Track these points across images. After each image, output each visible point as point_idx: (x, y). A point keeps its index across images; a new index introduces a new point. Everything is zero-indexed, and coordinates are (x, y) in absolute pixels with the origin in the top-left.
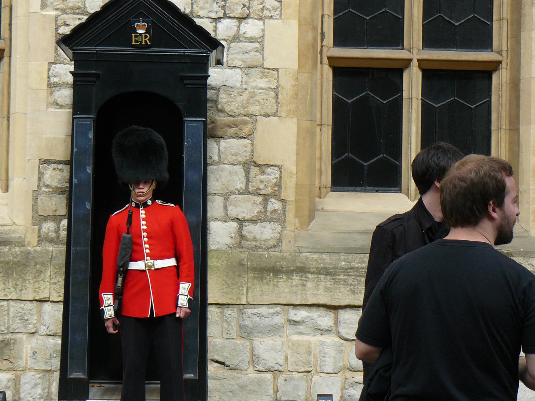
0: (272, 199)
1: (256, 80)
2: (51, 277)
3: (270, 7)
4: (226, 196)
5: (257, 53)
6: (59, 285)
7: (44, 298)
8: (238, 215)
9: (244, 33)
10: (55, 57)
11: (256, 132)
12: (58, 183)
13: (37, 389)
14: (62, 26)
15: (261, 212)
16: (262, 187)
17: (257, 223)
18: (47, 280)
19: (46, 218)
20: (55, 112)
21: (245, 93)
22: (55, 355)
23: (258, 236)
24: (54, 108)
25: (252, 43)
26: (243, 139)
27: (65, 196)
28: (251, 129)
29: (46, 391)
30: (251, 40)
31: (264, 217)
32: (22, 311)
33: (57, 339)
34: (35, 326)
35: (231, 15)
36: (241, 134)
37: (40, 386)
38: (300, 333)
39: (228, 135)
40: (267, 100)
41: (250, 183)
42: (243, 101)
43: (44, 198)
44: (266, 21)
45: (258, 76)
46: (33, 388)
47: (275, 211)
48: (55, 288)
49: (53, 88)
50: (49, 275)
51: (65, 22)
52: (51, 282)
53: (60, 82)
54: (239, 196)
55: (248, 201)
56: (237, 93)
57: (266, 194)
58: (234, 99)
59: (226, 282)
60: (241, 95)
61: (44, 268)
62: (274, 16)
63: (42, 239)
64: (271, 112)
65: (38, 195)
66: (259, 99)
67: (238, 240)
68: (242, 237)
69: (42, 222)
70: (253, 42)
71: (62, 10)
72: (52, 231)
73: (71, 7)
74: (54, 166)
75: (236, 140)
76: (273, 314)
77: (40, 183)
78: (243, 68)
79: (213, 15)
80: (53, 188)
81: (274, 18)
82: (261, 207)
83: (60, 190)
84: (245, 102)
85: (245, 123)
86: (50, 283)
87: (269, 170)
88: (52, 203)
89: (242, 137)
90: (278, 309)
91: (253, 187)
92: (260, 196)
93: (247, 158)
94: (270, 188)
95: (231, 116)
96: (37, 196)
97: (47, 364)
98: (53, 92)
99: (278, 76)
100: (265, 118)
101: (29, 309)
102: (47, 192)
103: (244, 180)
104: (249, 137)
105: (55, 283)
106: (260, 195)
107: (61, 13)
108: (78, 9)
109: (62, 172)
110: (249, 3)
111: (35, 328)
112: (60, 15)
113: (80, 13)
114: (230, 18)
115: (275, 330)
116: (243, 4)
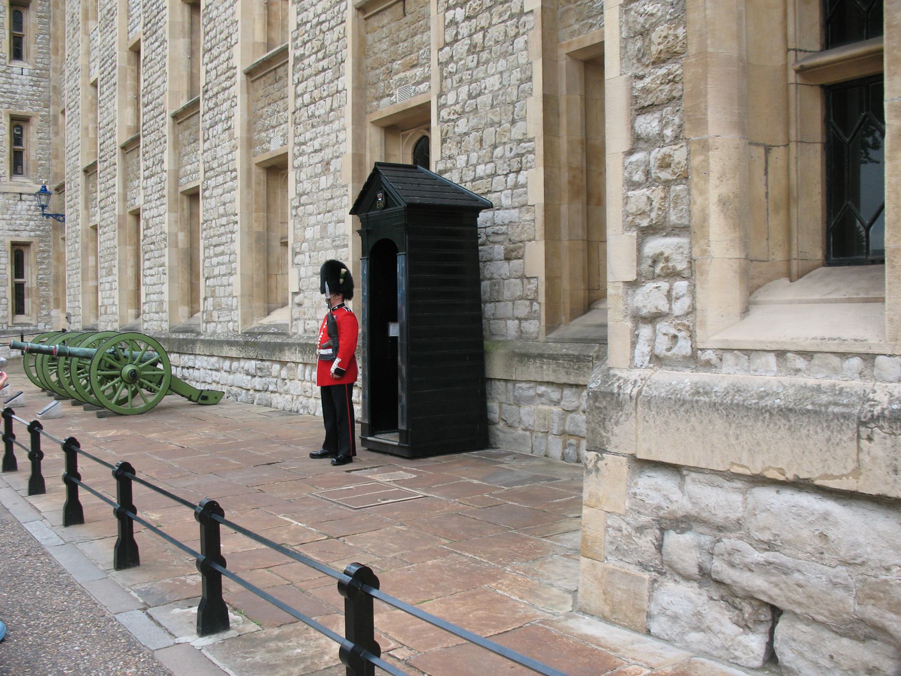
4: (513, 301)
38: (543, 404)
47: (535, 311)
68: (521, 331)
79: (505, 172)
85: (520, 248)
87: (532, 281)
90: (532, 385)
95: (514, 243)
114: (513, 172)
115: (530, 400)
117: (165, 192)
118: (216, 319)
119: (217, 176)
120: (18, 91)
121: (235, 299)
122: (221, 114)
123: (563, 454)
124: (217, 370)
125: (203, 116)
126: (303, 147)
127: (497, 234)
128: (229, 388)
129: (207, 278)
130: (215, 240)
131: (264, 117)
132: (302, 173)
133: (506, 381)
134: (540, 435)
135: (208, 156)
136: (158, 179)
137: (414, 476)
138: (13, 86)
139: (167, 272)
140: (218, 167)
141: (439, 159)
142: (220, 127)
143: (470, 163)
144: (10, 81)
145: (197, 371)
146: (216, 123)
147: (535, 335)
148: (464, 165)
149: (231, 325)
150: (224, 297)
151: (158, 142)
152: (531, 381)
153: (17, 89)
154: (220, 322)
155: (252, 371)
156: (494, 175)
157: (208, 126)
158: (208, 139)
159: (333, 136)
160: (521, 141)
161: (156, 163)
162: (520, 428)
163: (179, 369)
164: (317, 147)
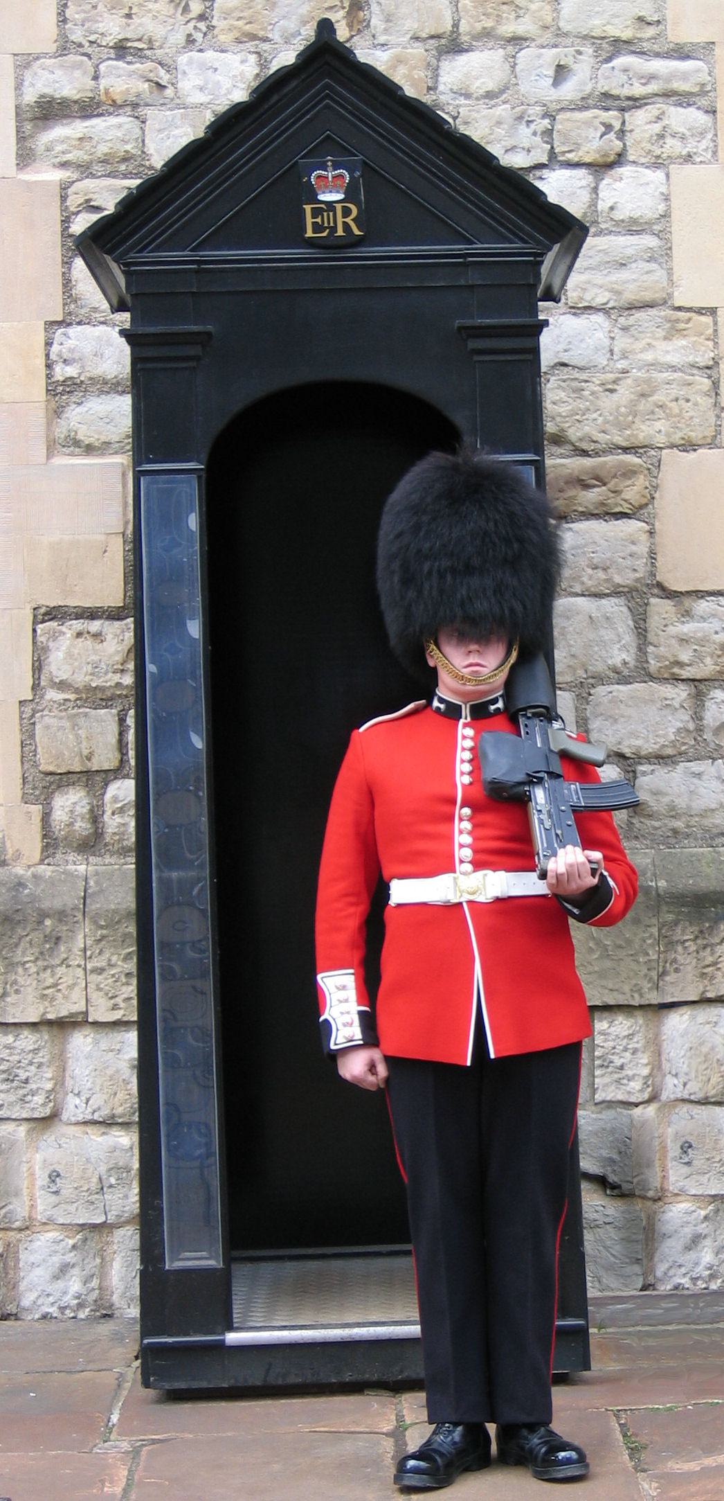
0: (716, 691)
1: (654, 343)
2: (89, 953)
3: (682, 130)
5: (654, 266)
6: (113, 976)
7: (72, 1015)
8: (620, 743)
9: (612, 208)
10: (64, 305)
11: (661, 497)
12: (91, 674)
13: (69, 1280)
14: (79, 212)
15: (688, 731)
16: (685, 657)
17: (675, 763)
18: (76, 963)
19: (62, 780)
20: (73, 465)
21: (621, 382)
22: (113, 1181)
23: (682, 803)
24: (69, 455)
25: (637, 237)
26: (624, 520)
27: (114, 711)
28: (647, 488)
29: (95, 1283)
30: (634, 227)
31: (697, 747)
32: (11, 1055)
33: (117, 1133)
34: (52, 1097)
35: (570, 156)
36: (617, 505)
37: (76, 1271)
39: (581, 509)
40: (688, 401)
41: (650, 649)
42: (618, 407)
43: (53, 722)
44: (673, 168)
45: (661, 333)
46: (56, 1277)
48: (102, 986)
49: (64, 397)
50: (83, 946)
51: (88, 201)
52: (89, 967)
53: (82, 379)
54: (621, 687)
55: (646, 702)
56: (599, 385)
57: (698, 677)
58: (591, 401)
59: (598, 942)
60: (612, 391)
61: (65, 928)
62: (695, 153)
63: (51, 843)
64: (700, 436)
65: (34, 712)
66: (663, 398)
69: (52, 793)
70: (638, 232)
71: (80, 166)
72: (82, 818)
73: (106, 155)
74: (78, 625)
75: (604, 523)
77: (39, 678)
78: (612, 311)
80: (77, 691)
81: (698, 160)
82: (687, 718)
83: (99, 696)
84: (623, 410)
85: (629, 473)
86: (85, 969)
87: (703, 606)
88: (77, 736)
89: (621, 513)
91: (659, 658)
92: (682, 686)
93: (637, 575)
94: (708, 660)
95: (584, 453)
96: (33, 716)
97: (92, 1208)
98: (63, 407)
99: (716, 331)
100: (685, 454)
101: (31, 1048)
102: (60, 705)
103: (629, 638)
104: (642, 512)
105: (100, 971)
106: (683, 680)
107: (75, 176)
108: (125, 160)
109: (102, 641)
110: (621, 121)
111: (51, 1104)
112: (74, 182)
113: (131, 173)
116: (603, 124)
160: (619, 46)
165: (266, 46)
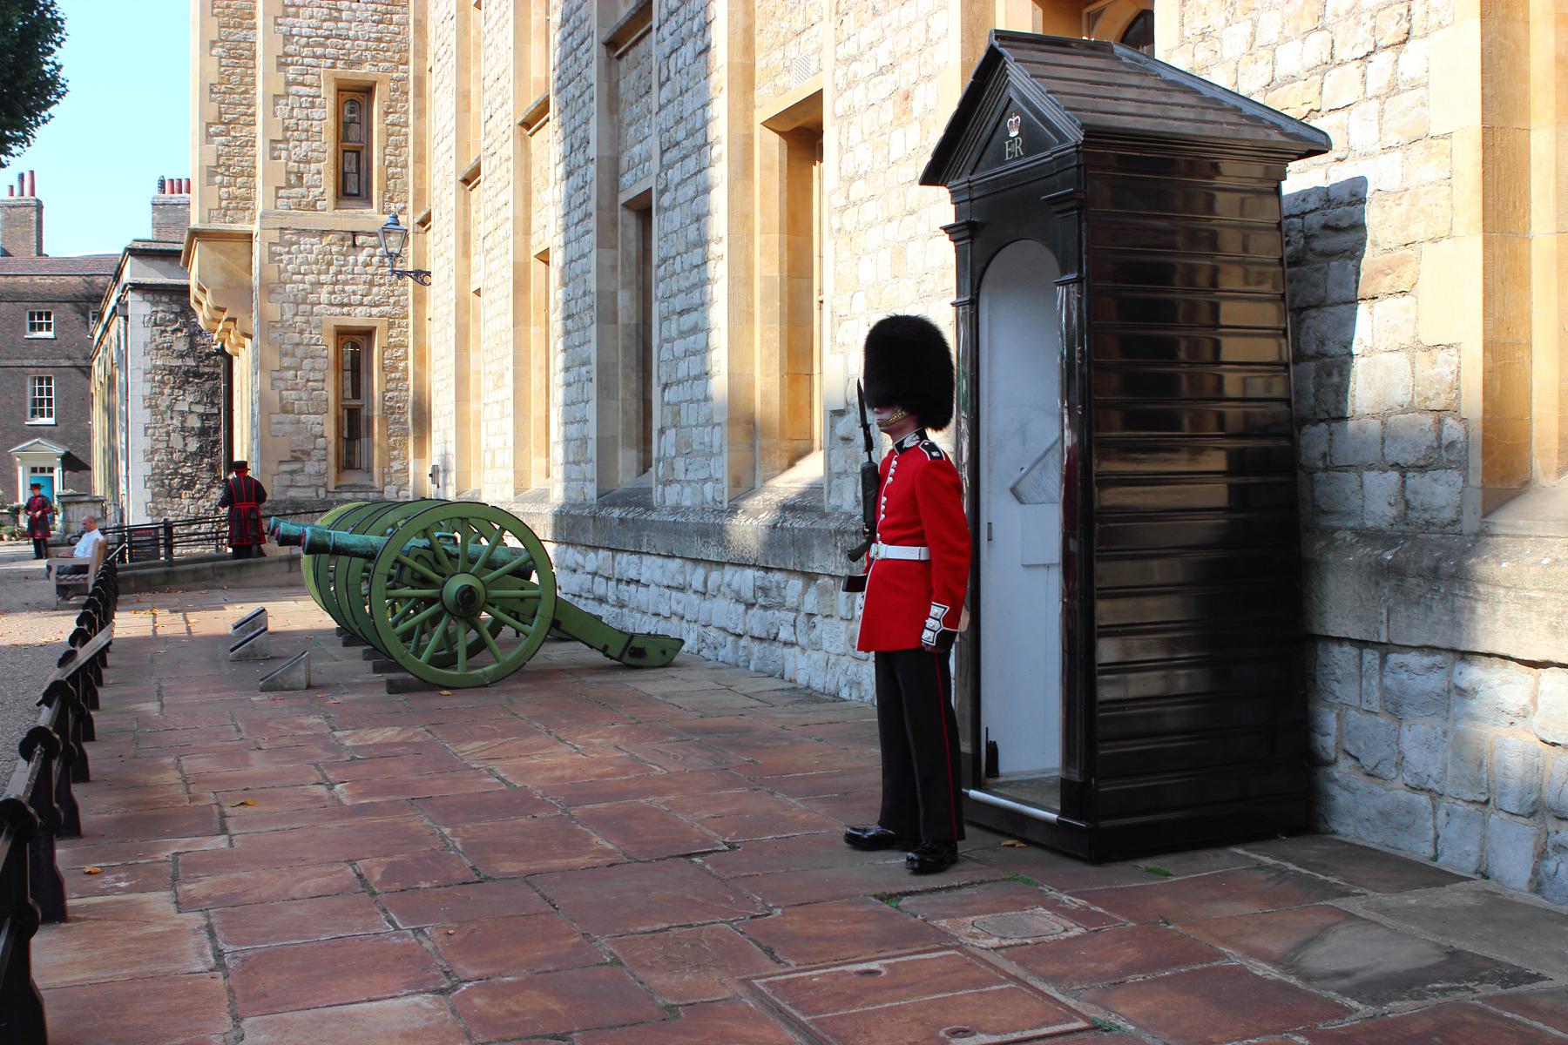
67: (1402, 507)
68: (1407, 503)
76: (1430, 668)
85: (1405, 261)
90: (1439, 659)
117: (592, 206)
118: (682, 477)
119: (685, 157)
120: (351, 33)
121: (717, 429)
122: (692, 19)
123: (1535, 872)
124: (681, 589)
125: (658, 29)
126: (856, 66)
127: (1337, 229)
128: (701, 630)
129: (666, 386)
130: (679, 303)
131: (778, 14)
132: (852, 128)
133: (1362, 644)
134: (1461, 807)
135: (667, 118)
136: (581, 178)
137: (1077, 931)
138: (340, 25)
139: (594, 375)
140: (687, 138)
141: (1176, 44)
142: (688, 50)
143: (1259, 42)
144: (336, 14)
145: (645, 589)
146: (683, 42)
147: (1449, 514)
148: (1244, 48)
149: (708, 487)
150: (698, 425)
151: (580, 101)
152: (1433, 649)
153: (350, 29)
154: (689, 482)
155: (748, 595)
156: (1331, 62)
157: (667, 51)
158: (668, 79)
159: (921, 26)
161: (576, 146)
162: (1399, 783)
163: (612, 583)
164: (884, 60)
165: (1254, 13)
